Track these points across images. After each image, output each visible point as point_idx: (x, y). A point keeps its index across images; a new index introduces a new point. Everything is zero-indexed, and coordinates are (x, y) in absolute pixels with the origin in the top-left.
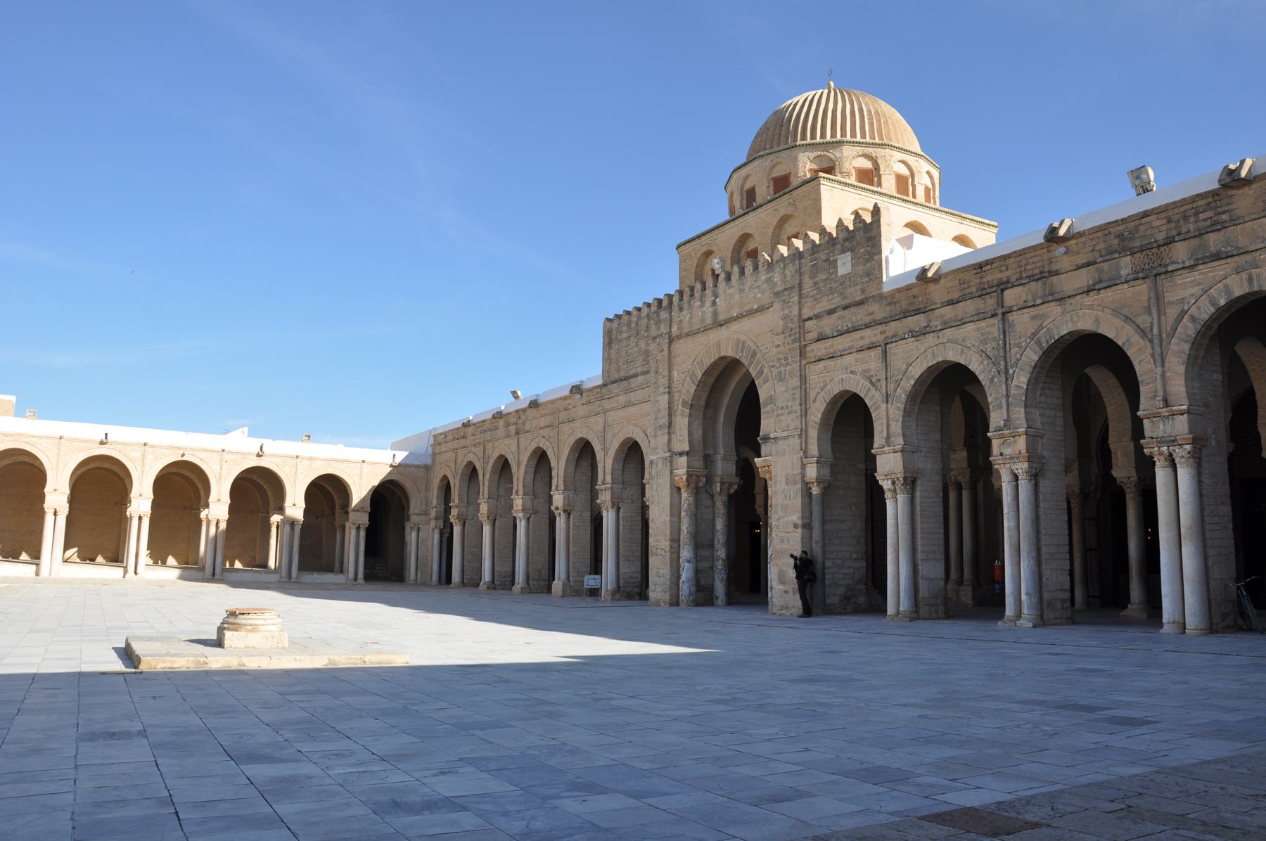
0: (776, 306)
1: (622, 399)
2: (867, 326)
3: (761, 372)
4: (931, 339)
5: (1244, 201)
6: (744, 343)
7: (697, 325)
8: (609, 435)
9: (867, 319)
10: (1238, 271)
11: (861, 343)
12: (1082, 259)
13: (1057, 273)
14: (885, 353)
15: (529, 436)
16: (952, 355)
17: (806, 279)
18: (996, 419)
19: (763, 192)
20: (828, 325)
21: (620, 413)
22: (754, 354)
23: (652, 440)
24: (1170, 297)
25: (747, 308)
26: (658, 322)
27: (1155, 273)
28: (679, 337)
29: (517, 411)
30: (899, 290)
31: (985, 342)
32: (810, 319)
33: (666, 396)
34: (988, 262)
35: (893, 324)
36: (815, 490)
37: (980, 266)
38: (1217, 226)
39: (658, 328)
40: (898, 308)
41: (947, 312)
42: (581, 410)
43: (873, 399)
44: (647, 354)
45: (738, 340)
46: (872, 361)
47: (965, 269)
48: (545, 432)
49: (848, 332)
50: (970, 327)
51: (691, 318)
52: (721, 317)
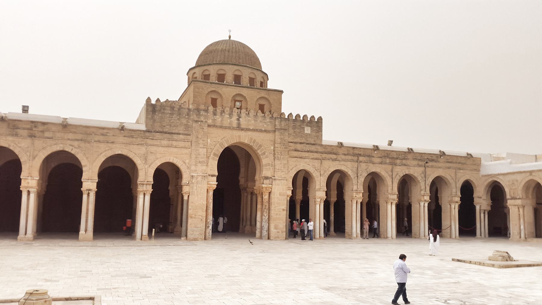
0: (277, 133)
1: (165, 142)
2: (316, 152)
3: (264, 153)
4: (337, 162)
5: (410, 156)
6: (255, 141)
7: (226, 123)
8: (151, 158)
9: (316, 150)
10: (407, 169)
11: (313, 157)
12: (379, 156)
13: (373, 157)
14: (321, 162)
15: (49, 142)
16: (343, 168)
17: (290, 129)
18: (355, 188)
19: (245, 81)
20: (299, 147)
21: (161, 149)
22: (261, 146)
23: (193, 168)
24: (395, 170)
25: (260, 128)
26: (199, 115)
27: (393, 164)
28: (214, 126)
29: (32, 122)
30: (328, 146)
31: (353, 167)
32: (292, 142)
33: (205, 150)
34: (356, 148)
35: (325, 155)
36: (289, 199)
37: (354, 148)
38: (404, 159)
39: (199, 118)
40: (327, 151)
41: (343, 157)
42: (121, 139)
43: (315, 174)
44: (187, 127)
45: (251, 139)
46: (317, 163)
47: (350, 147)
48: (76, 143)
49: (308, 151)
50: (349, 163)
51: (222, 120)
52: (242, 127)
